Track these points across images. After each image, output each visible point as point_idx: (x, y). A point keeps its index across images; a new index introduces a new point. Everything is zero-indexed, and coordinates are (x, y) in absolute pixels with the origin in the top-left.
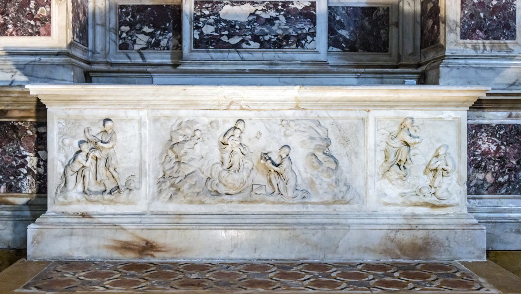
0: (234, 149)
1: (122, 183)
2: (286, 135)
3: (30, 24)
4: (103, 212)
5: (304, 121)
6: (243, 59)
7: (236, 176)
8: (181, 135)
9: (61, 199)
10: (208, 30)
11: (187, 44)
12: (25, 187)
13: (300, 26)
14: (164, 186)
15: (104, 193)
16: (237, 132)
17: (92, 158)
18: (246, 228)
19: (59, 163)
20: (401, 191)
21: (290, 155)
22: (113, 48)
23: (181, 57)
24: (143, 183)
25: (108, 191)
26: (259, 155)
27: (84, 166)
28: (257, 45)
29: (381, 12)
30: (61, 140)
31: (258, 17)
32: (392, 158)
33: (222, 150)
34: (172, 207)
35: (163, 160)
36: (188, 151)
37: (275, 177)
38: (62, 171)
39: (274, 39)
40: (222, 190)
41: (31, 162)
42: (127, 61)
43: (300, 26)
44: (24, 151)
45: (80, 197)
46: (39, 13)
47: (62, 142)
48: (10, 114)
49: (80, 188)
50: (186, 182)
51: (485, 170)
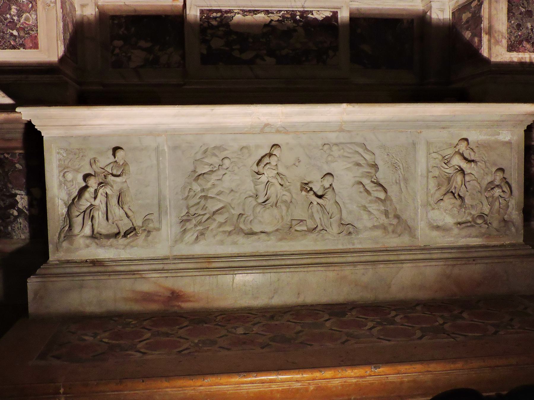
0: (270, 179)
3: (12, 35)
4: (116, 257)
5: (348, 145)
8: (207, 164)
10: (217, 43)
12: (17, 232)
14: (189, 226)
15: (118, 236)
16: (273, 160)
17: (101, 194)
18: (288, 270)
19: (61, 203)
21: (334, 185)
24: (164, 222)
25: (122, 234)
26: (299, 185)
27: (91, 205)
30: (62, 174)
34: (199, 249)
35: (186, 194)
36: (217, 183)
37: (318, 211)
38: (65, 210)
41: (22, 201)
44: (12, 188)
46: (22, 20)
47: (64, 176)
50: (215, 220)
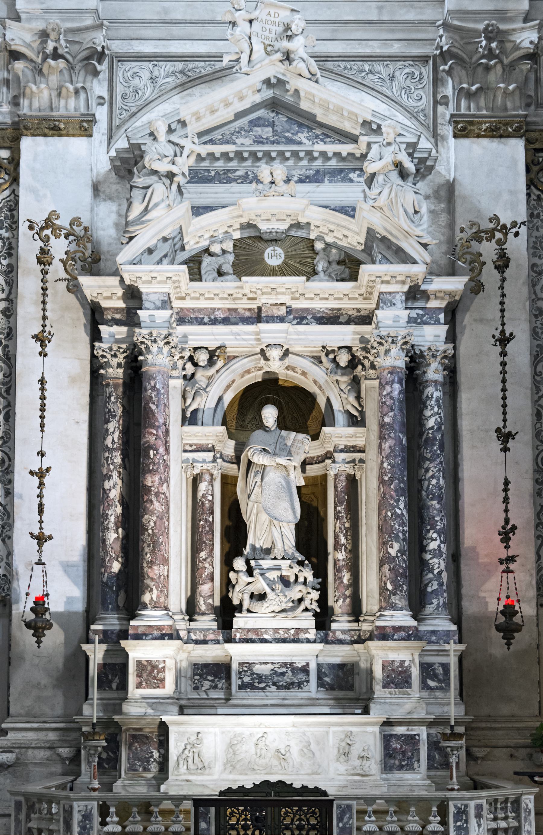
1: (206, 765)
2: (288, 740)
6: (267, 696)
7: (263, 761)
9: (176, 773)
10: (247, 679)
11: (234, 687)
13: (300, 676)
16: (264, 738)
20: (346, 768)
22: (189, 689)
23: (230, 694)
28: (275, 688)
29: (349, 667)
31: (276, 672)
32: (341, 751)
33: (256, 748)
38: (176, 758)
39: (285, 684)
40: (256, 767)
42: (198, 697)
43: (300, 676)
45: (186, 771)
48: (144, 730)
49: (185, 767)
51: (395, 758)
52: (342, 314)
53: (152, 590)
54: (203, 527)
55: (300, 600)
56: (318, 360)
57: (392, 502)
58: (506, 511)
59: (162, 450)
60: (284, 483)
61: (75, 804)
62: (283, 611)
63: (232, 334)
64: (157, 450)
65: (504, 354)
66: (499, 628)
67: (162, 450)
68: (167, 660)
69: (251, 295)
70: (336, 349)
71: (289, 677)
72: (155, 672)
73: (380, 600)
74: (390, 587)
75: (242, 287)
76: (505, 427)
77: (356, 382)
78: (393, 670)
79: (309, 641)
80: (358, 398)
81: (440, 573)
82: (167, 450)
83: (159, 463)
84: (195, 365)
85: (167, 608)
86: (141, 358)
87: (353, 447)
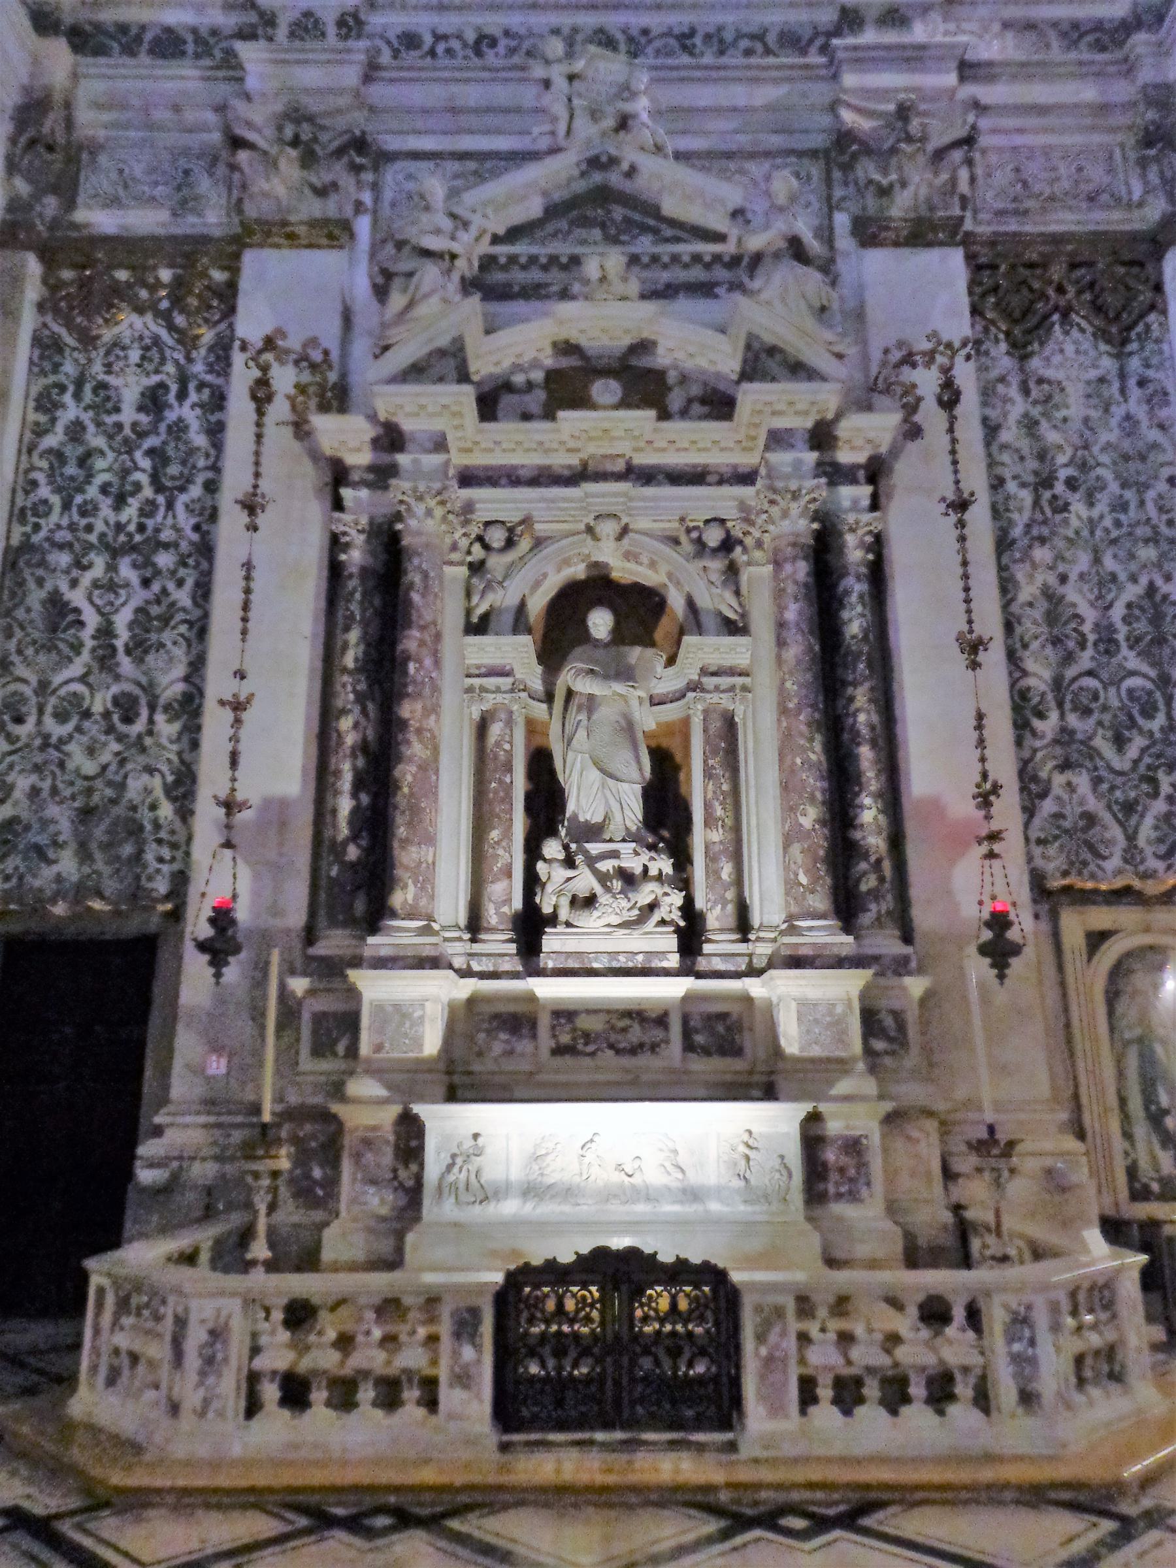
10: (565, 1039)
39: (628, 1046)
52: (709, 473)
53: (405, 887)
54: (496, 792)
55: (652, 907)
56: (676, 542)
57: (802, 742)
58: (983, 760)
59: (428, 662)
60: (623, 723)
61: (194, 1304)
62: (625, 925)
63: (543, 500)
64: (419, 661)
65: (961, 524)
66: (984, 950)
67: (428, 662)
68: (427, 1004)
69: (572, 444)
70: (701, 524)
71: (636, 1034)
72: (407, 1025)
73: (787, 903)
74: (803, 879)
75: (558, 431)
76: (971, 631)
77: (732, 570)
78: (816, 1021)
79: (666, 973)
80: (737, 593)
81: (879, 861)
82: (437, 663)
83: (423, 683)
84: (486, 547)
85: (431, 918)
86: (399, 526)
87: (731, 668)
